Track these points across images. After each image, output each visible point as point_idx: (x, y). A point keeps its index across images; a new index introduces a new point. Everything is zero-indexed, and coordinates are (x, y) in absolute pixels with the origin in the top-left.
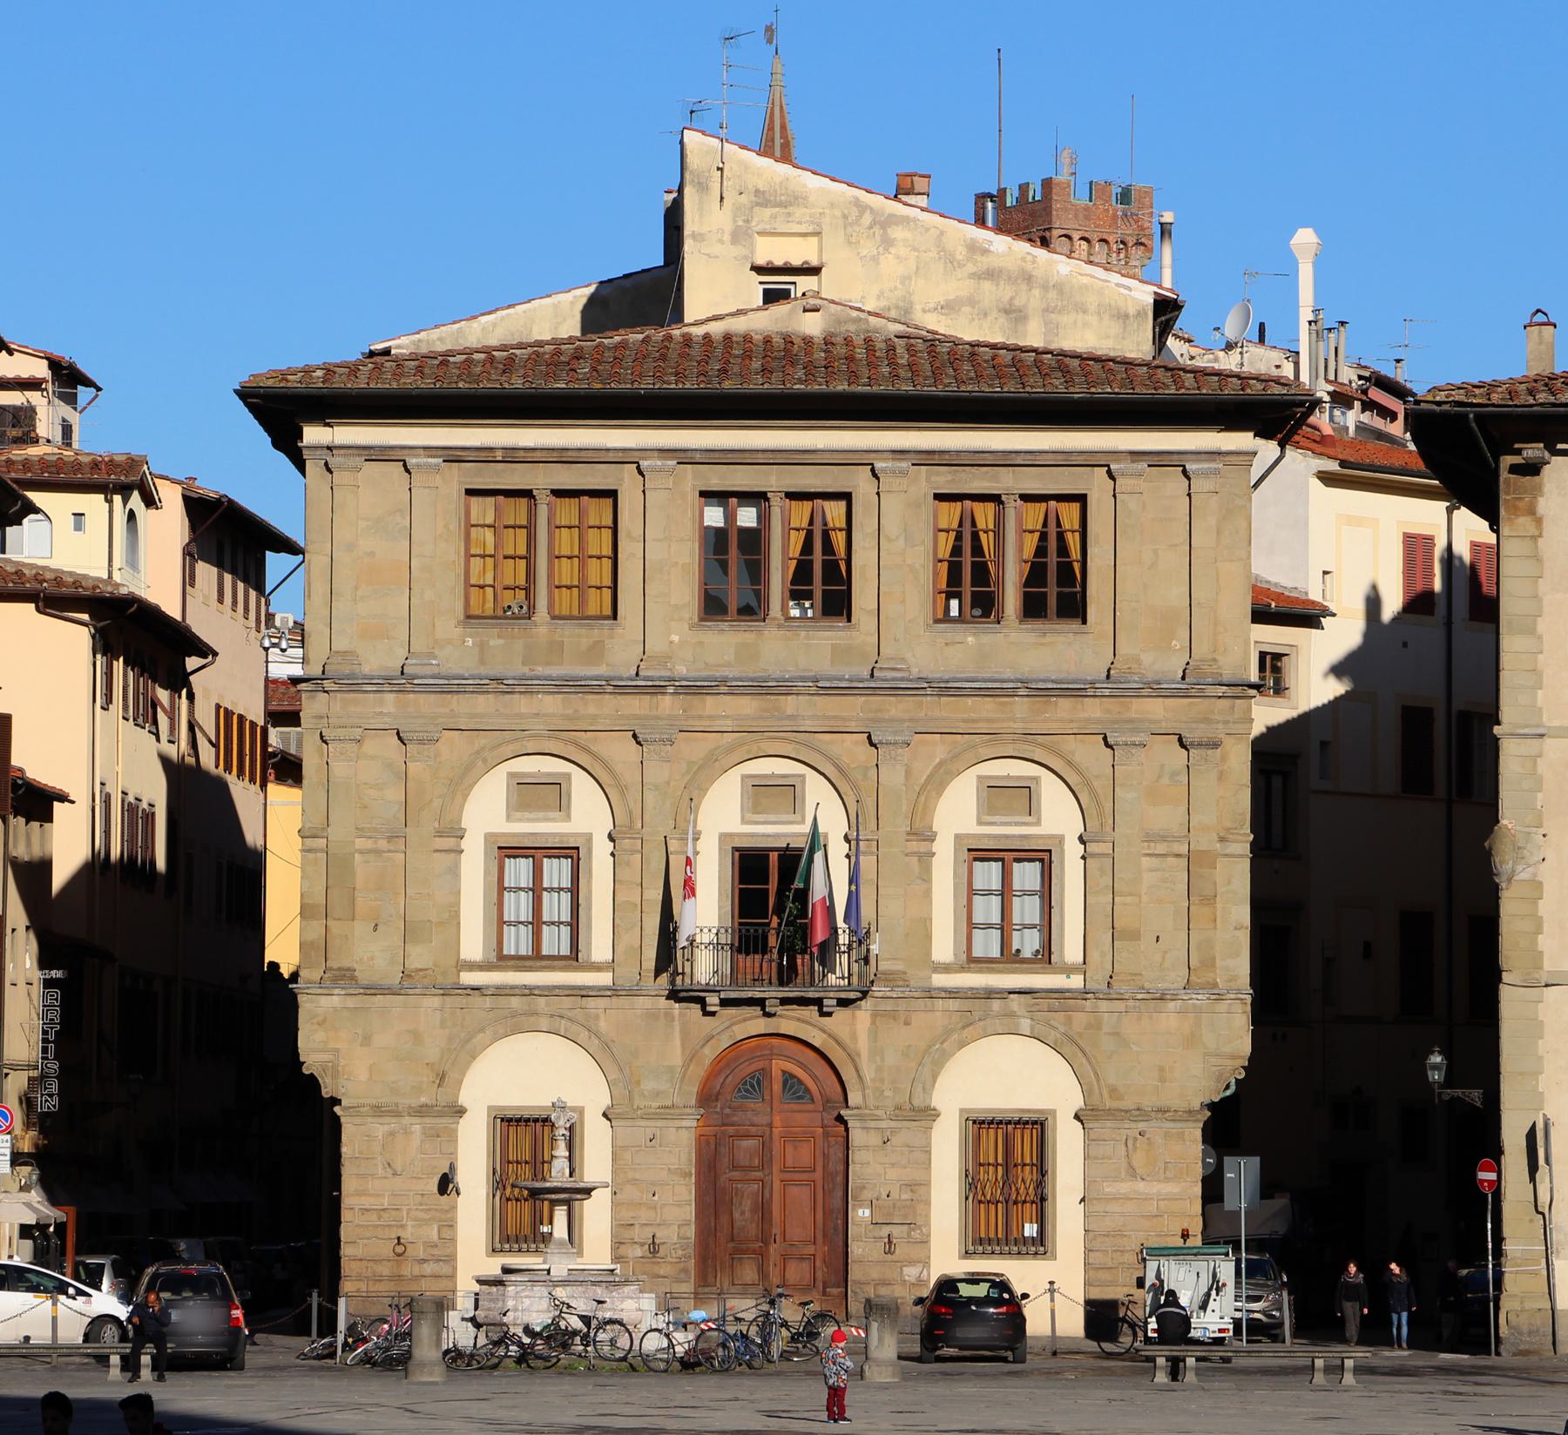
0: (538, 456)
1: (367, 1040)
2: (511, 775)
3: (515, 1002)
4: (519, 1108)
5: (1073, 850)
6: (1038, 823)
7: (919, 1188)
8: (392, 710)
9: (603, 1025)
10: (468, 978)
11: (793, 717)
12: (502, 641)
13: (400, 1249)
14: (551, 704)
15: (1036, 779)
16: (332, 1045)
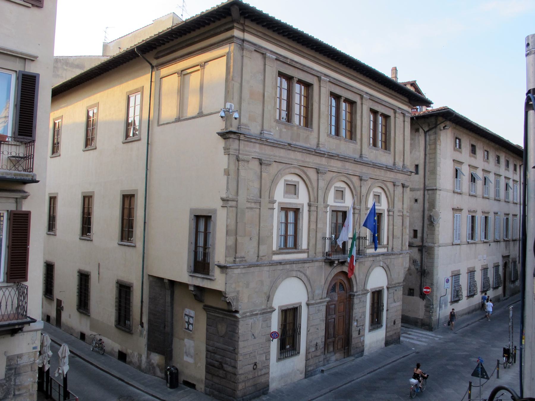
0: (298, 66)
1: (247, 285)
2: (285, 181)
3: (288, 266)
4: (286, 306)
5: (386, 213)
6: (381, 206)
7: (364, 313)
8: (258, 151)
9: (308, 273)
10: (276, 258)
11: (348, 169)
12: (285, 130)
13: (255, 367)
14: (298, 156)
15: (381, 193)
16: (238, 289)
